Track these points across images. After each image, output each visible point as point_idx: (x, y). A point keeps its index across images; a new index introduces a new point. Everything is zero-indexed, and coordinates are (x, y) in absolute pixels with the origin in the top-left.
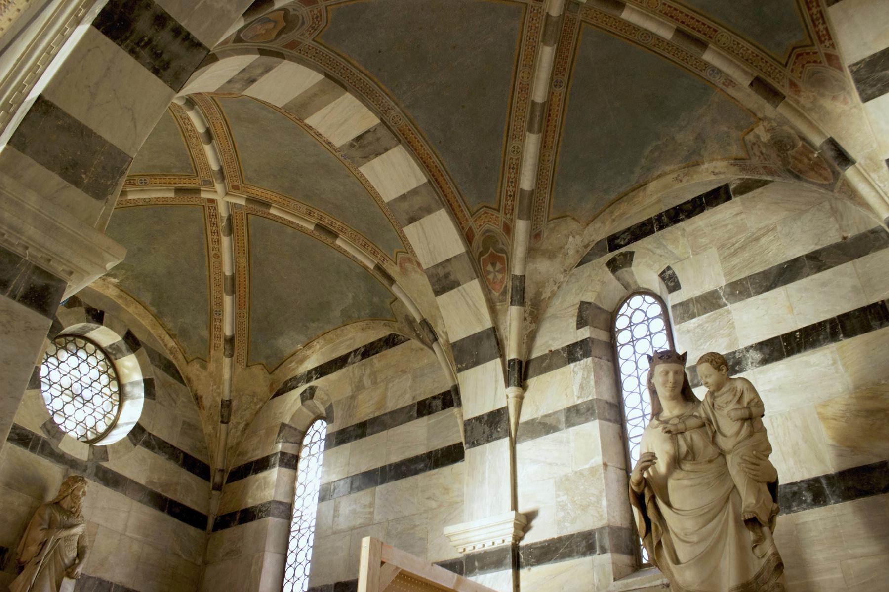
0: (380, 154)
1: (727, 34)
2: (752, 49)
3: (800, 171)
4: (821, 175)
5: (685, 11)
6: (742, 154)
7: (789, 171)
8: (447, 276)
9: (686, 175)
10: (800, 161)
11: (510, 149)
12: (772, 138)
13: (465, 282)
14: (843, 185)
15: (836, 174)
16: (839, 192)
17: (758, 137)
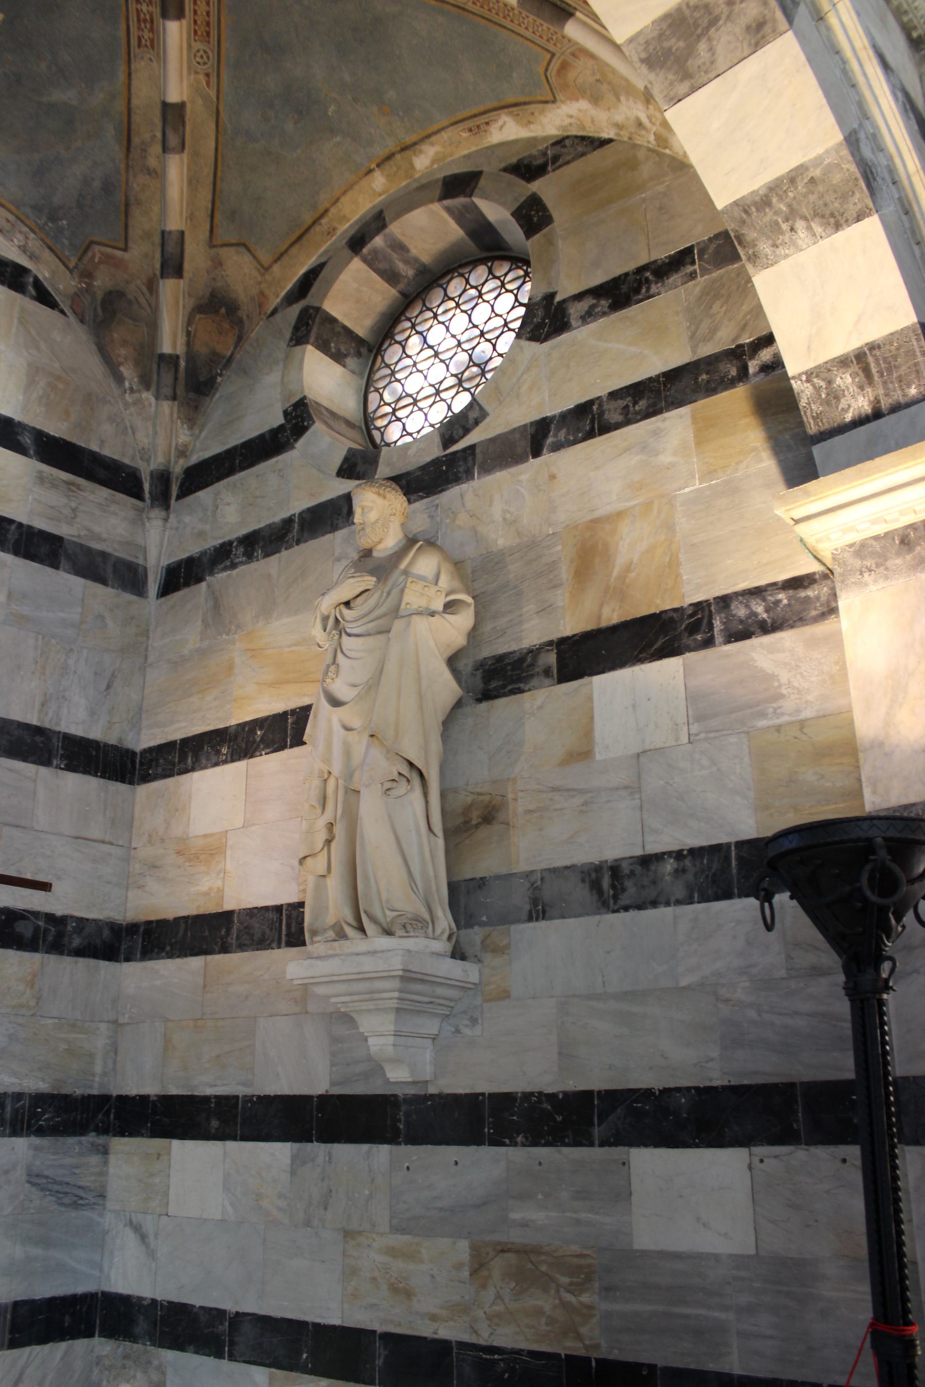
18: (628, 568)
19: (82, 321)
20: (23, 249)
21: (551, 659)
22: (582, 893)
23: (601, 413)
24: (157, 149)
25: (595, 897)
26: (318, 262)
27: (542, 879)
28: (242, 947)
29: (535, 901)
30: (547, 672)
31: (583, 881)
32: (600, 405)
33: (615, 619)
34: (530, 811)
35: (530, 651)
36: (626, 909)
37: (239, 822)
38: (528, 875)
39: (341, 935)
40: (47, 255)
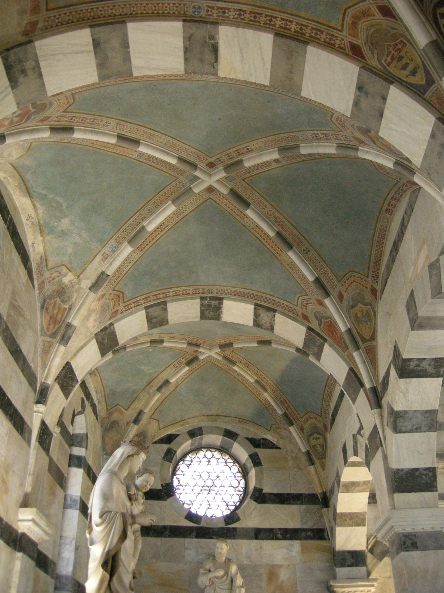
0: (185, 52)
1: (138, 257)
2: (126, 270)
3: (47, 309)
4: (49, 324)
5: (159, 236)
6: (51, 264)
7: (45, 301)
8: (24, 72)
9: (33, 224)
10: (54, 307)
11: (110, 120)
12: (66, 286)
13: (15, 96)
14: (49, 342)
15: (54, 335)
16: (42, 341)
17: (66, 275)
18: (283, 582)
19: (102, 426)
20: (98, 399)
23: (276, 534)
26: (175, 433)
40: (104, 403)
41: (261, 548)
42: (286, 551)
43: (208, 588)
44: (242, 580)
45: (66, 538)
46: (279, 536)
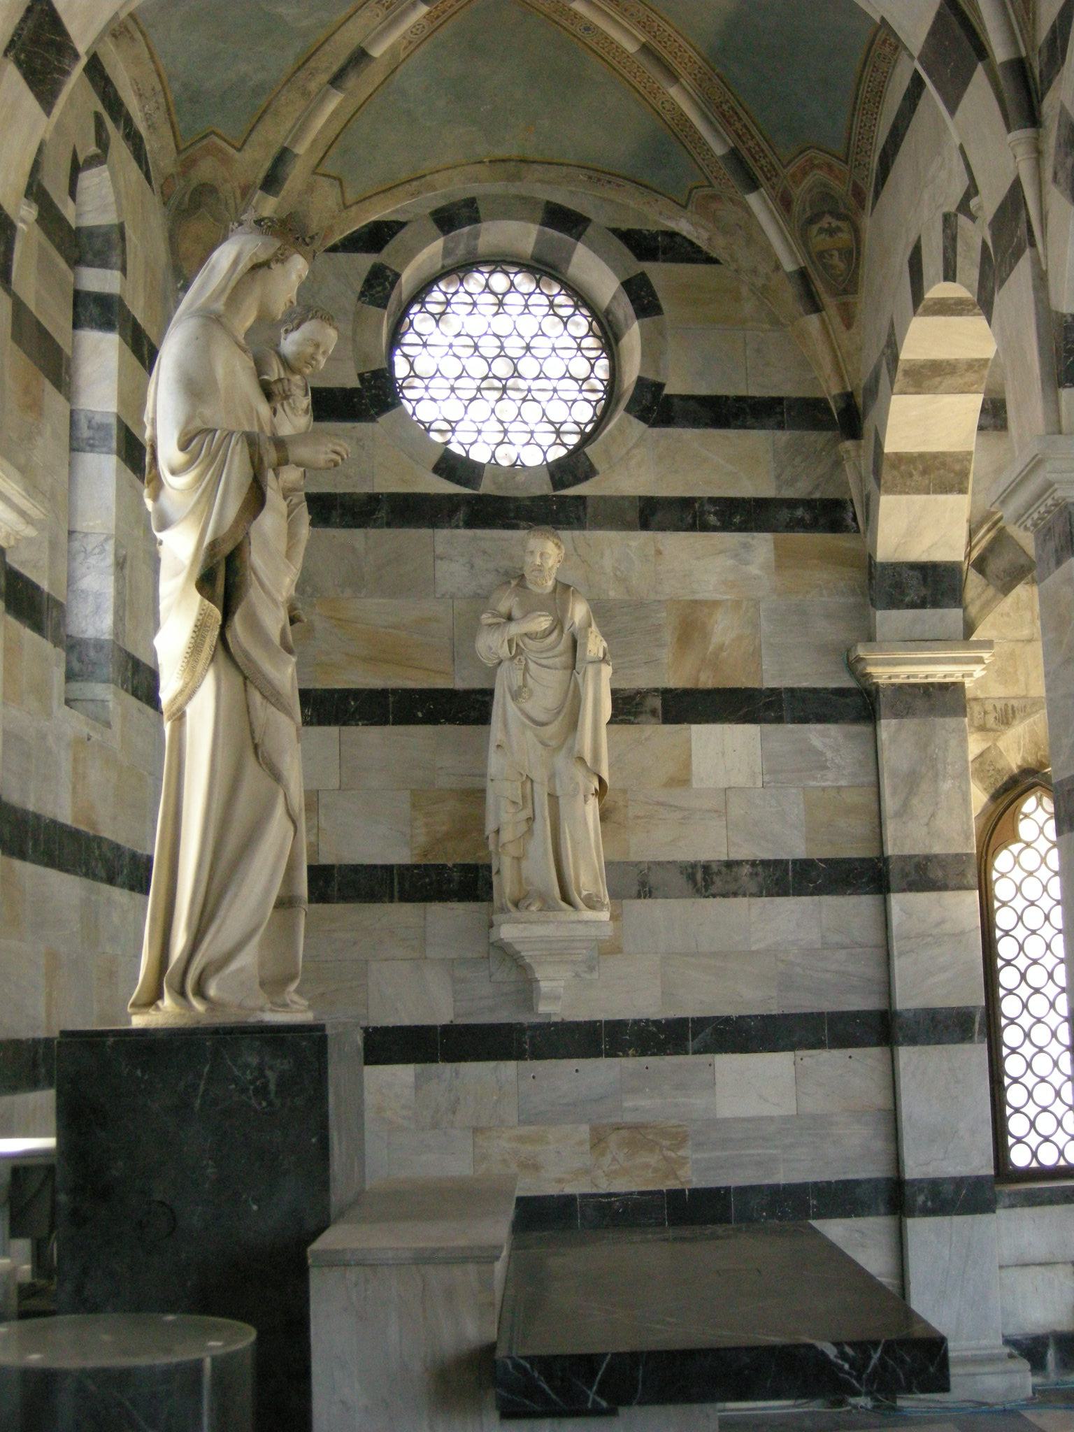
18: (721, 648)
19: (165, 204)
20: (148, 117)
21: (657, 703)
22: (681, 881)
23: (703, 513)
24: (325, 77)
25: (691, 886)
26: (393, 218)
27: (649, 868)
28: (345, 899)
29: (643, 884)
30: (653, 712)
31: (682, 873)
32: (702, 505)
33: (710, 685)
34: (638, 817)
35: (639, 692)
36: (714, 896)
37: (334, 783)
38: (638, 864)
39: (547, 906)
40: (166, 130)
41: (659, 553)
42: (730, 562)
43: (506, 664)
44: (605, 644)
45: (86, 535)
46: (712, 519)
